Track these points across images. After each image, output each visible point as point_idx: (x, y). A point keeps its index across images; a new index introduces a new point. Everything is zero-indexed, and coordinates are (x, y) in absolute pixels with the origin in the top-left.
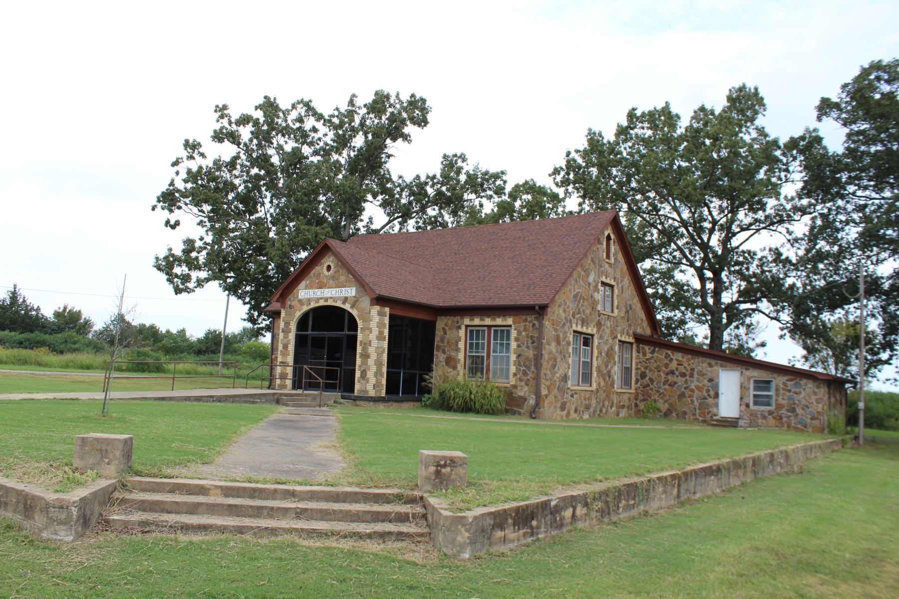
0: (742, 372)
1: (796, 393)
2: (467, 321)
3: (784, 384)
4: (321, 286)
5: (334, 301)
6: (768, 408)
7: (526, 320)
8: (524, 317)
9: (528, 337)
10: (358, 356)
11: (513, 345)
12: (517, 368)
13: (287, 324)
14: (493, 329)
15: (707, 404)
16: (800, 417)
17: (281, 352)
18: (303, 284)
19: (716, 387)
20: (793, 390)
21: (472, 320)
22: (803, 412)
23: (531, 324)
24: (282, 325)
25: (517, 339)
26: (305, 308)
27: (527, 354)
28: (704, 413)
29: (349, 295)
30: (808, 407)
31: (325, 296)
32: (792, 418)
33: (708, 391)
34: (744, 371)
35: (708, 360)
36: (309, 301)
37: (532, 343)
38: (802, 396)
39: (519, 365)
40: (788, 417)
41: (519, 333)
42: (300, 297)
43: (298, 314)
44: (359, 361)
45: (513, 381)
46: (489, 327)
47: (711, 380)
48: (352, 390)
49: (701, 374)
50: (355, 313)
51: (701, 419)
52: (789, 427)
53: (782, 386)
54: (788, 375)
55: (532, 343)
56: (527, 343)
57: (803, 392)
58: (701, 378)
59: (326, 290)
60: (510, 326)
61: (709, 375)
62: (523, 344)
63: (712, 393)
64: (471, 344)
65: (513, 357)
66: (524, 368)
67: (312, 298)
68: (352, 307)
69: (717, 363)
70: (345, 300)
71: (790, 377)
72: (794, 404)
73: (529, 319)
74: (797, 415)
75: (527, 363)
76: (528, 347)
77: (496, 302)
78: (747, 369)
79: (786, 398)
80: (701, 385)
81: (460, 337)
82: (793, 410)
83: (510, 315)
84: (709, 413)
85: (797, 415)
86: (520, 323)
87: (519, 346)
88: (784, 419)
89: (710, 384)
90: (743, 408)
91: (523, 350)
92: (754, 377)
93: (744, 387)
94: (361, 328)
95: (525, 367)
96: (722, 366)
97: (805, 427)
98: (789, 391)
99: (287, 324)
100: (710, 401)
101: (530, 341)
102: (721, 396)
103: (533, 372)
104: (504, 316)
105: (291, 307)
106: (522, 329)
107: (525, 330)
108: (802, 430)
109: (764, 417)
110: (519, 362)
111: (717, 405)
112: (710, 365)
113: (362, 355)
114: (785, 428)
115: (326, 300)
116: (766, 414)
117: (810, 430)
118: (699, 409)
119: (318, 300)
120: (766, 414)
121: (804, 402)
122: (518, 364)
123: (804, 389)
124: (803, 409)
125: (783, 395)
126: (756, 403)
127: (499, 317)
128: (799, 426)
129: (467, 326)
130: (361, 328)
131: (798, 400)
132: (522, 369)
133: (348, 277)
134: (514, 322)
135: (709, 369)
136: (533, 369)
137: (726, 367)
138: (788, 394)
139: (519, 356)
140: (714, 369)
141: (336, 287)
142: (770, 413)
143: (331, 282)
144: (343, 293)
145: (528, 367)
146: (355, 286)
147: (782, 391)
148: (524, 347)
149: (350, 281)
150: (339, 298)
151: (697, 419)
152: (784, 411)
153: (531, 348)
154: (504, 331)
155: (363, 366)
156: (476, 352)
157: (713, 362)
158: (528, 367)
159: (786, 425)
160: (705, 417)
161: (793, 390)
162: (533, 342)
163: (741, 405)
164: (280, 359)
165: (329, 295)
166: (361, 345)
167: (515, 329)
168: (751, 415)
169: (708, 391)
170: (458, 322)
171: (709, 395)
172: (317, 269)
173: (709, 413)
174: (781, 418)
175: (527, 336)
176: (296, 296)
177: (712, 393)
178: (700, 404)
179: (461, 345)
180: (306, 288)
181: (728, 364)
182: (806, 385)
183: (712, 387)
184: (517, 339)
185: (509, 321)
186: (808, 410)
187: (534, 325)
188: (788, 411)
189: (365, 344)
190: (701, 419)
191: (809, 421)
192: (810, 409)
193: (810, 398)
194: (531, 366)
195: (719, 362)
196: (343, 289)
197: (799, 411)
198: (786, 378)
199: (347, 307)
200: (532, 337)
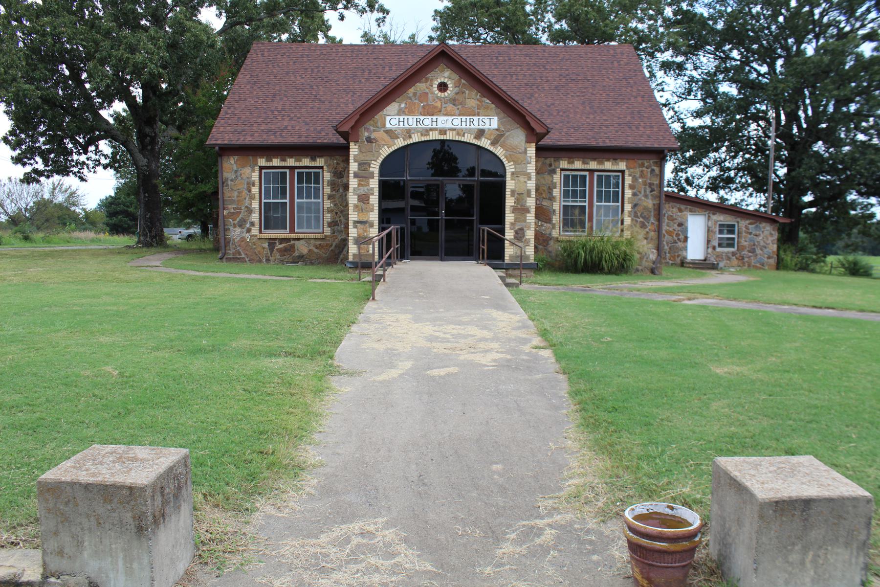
0: (709, 217)
1: (756, 236)
2: (564, 164)
3: (746, 227)
4: (430, 111)
5: (458, 134)
6: (731, 250)
7: (643, 165)
8: (640, 162)
9: (645, 185)
10: (508, 211)
11: (628, 193)
12: (632, 220)
13: (364, 165)
14: (296, 171)
15: (677, 248)
16: (759, 256)
17: (356, 206)
18: (393, 107)
19: (685, 231)
20: (754, 233)
21: (270, 160)
22: (761, 252)
23: (649, 170)
24: (353, 166)
25: (631, 187)
26: (400, 143)
27: (645, 204)
28: (674, 257)
29: (487, 126)
30: (765, 247)
31: (440, 125)
32: (752, 258)
33: (678, 235)
34: (711, 215)
35: (678, 205)
36: (409, 133)
37: (651, 192)
38: (761, 238)
39: (636, 216)
40: (749, 257)
41: (635, 179)
42: (388, 125)
43: (386, 151)
44: (509, 217)
45: (627, 234)
46: (292, 168)
47: (680, 225)
48: (500, 255)
49: (671, 219)
50: (499, 151)
51: (671, 262)
52: (749, 266)
53: (744, 229)
54: (750, 219)
55: (651, 192)
56: (645, 191)
57: (762, 235)
58: (671, 223)
59: (441, 119)
60: (322, 168)
61: (680, 220)
62: (640, 192)
63: (682, 237)
64: (599, 193)
65: (628, 207)
66: (641, 219)
67: (414, 129)
68: (494, 143)
69: (686, 208)
70: (480, 133)
71: (751, 221)
72: (754, 245)
73: (646, 164)
74: (756, 255)
75: (645, 214)
76: (646, 196)
77: (608, 143)
78: (714, 214)
79: (747, 240)
80: (671, 229)
81: (556, 183)
82: (753, 251)
83: (622, 159)
84: (678, 256)
85: (756, 255)
86: (634, 168)
87: (634, 194)
88: (746, 259)
89: (679, 228)
90: (710, 250)
91: (640, 199)
92: (721, 221)
93: (712, 231)
94: (513, 173)
95: (643, 218)
96: (691, 211)
97: (763, 265)
98: (750, 233)
99: (364, 165)
100: (680, 244)
101: (648, 190)
102: (689, 240)
103: (653, 223)
104: (615, 159)
105: (369, 140)
106: (638, 175)
107: (641, 176)
108: (760, 268)
109: (729, 259)
110: (635, 212)
111: (685, 249)
112: (680, 210)
113: (515, 210)
114: (746, 267)
115: (443, 132)
116: (730, 255)
117: (766, 268)
118: (669, 253)
119: (427, 131)
120: (730, 255)
121: (762, 243)
122: (634, 214)
123: (763, 232)
124: (761, 250)
125: (745, 237)
126: (720, 245)
127: (608, 160)
128: (758, 265)
129: (261, 168)
130: (513, 173)
131: (758, 242)
132: (639, 220)
133: (481, 102)
134: (325, 163)
135: (679, 214)
136: (652, 220)
137: (695, 212)
138: (749, 236)
139: (635, 206)
140: (683, 213)
141: (459, 115)
142: (734, 254)
143: (450, 107)
144: (476, 123)
145: (646, 218)
146: (497, 115)
147: (744, 234)
148: (641, 196)
149: (487, 108)
150: (469, 131)
151: (668, 263)
152: (745, 252)
153: (650, 197)
154: (609, 176)
155: (518, 224)
156: (572, 201)
157: (683, 207)
158: (646, 218)
159: (746, 264)
160: (675, 260)
161: (754, 233)
162: (652, 191)
163: (708, 248)
164: (353, 216)
165: (449, 125)
166: (512, 195)
167: (630, 175)
168: (717, 256)
169: (678, 235)
170: (550, 165)
171: (679, 239)
172: (420, 87)
173: (678, 256)
174: (743, 258)
175: (645, 183)
176: (379, 125)
177: (682, 237)
178: (670, 248)
179: (556, 193)
180: (400, 112)
181: (697, 209)
182: (764, 228)
183: (682, 232)
184: (631, 187)
185: (622, 166)
186: (765, 250)
187: (653, 171)
188: (749, 251)
189: (520, 194)
190: (671, 262)
191: (766, 260)
192: (767, 250)
193: (767, 239)
194: (650, 217)
195: (689, 207)
196: (476, 118)
197: (758, 251)
198: (748, 222)
199: (485, 143)
200: (651, 185)
